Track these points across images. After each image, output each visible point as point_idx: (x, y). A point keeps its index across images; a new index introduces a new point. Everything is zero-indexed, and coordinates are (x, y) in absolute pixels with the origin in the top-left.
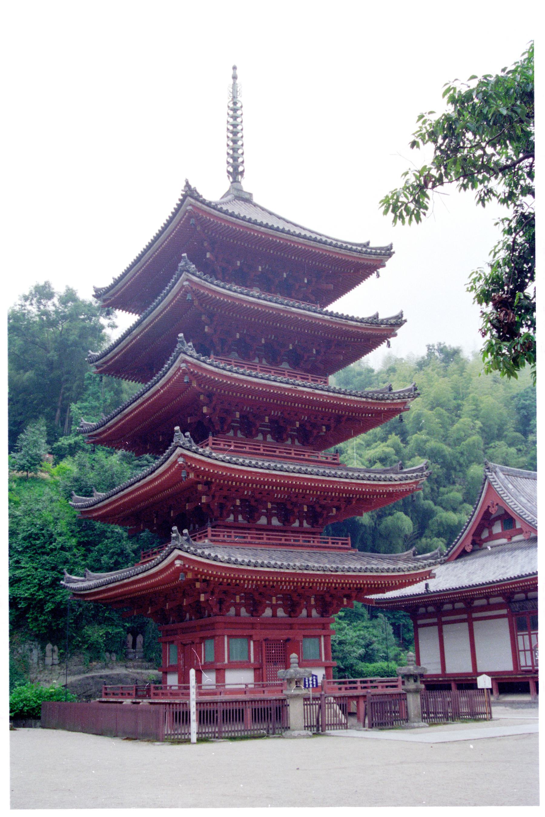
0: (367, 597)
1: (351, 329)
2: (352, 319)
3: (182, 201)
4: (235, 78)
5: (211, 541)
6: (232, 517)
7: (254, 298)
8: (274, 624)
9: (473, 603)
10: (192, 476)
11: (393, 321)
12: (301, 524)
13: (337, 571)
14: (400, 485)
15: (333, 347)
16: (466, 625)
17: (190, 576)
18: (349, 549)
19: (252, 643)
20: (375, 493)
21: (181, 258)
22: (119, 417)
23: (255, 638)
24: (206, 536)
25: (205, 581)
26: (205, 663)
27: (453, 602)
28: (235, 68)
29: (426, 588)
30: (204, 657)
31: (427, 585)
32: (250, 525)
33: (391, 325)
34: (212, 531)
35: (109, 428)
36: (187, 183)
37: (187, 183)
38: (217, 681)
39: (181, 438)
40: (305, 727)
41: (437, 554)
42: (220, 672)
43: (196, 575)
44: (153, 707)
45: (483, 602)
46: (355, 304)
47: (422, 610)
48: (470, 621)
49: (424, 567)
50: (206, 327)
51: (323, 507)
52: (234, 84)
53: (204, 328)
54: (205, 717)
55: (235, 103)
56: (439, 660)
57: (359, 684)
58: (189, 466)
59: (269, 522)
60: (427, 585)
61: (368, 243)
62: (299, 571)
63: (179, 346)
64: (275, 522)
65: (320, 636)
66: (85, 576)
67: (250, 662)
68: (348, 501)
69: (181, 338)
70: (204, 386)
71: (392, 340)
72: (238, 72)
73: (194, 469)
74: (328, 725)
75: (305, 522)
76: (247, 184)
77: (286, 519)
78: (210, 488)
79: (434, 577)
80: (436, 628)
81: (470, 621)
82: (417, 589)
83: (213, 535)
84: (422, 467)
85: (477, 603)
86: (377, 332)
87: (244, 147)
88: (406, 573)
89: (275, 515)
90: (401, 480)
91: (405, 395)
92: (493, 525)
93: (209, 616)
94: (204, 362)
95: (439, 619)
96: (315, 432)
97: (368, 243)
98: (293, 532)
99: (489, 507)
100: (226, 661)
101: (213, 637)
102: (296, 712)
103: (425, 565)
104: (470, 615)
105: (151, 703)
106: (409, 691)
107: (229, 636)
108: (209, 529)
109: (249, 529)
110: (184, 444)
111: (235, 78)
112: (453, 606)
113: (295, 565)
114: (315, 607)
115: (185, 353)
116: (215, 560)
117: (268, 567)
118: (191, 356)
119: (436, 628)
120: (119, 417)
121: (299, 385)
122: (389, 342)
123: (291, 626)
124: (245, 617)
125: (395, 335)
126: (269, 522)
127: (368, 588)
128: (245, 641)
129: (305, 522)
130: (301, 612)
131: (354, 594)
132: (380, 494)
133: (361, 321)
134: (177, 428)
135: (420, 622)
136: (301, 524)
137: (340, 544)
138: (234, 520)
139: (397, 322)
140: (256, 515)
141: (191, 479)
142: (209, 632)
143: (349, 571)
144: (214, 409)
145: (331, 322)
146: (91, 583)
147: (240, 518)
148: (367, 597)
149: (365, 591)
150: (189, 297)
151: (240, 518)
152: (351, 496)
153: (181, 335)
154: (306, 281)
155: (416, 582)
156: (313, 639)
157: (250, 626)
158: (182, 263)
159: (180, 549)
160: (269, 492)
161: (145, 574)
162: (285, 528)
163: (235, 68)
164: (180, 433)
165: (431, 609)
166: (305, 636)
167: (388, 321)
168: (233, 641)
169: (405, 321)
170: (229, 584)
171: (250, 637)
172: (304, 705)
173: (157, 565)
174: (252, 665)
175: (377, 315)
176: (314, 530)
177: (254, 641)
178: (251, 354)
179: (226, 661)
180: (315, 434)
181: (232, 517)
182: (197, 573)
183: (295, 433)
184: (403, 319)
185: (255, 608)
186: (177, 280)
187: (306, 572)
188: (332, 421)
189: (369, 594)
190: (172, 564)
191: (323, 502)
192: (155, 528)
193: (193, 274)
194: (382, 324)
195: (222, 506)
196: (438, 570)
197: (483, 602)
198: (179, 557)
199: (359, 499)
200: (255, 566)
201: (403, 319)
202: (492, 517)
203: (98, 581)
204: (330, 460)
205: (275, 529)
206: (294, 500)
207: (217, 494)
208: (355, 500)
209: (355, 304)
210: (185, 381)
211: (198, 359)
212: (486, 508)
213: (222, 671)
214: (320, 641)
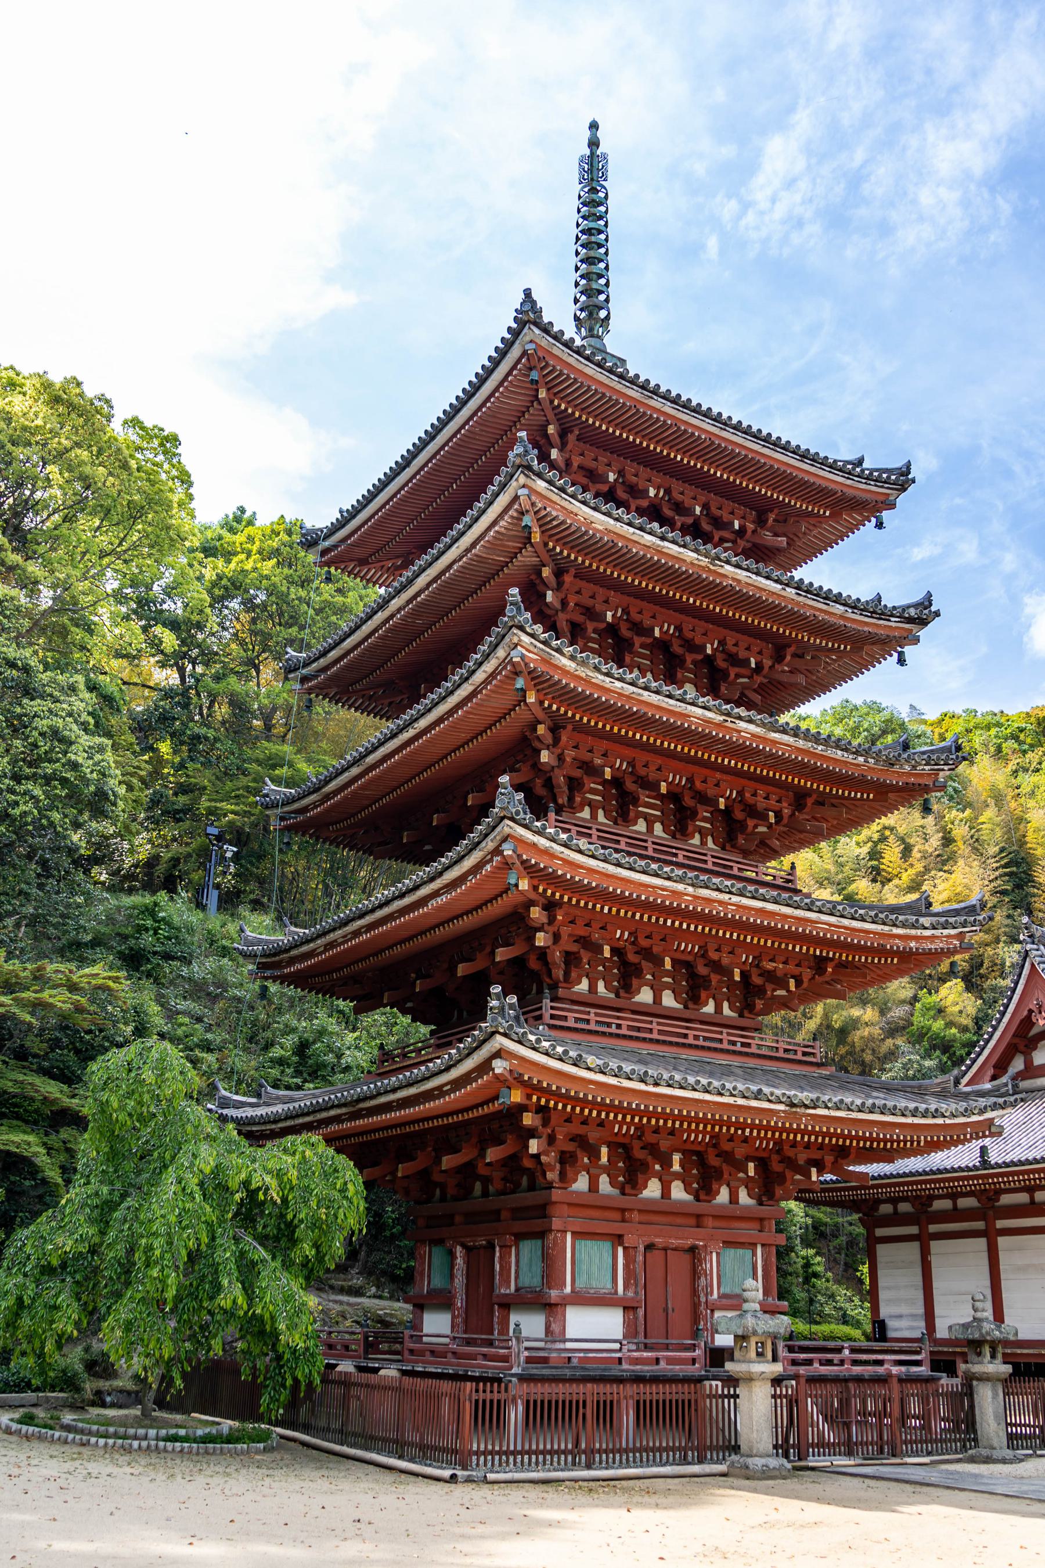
0: (851, 1168)
1: (833, 620)
2: (838, 599)
3: (515, 333)
4: (594, 143)
5: (552, 1027)
6: (584, 985)
7: (647, 540)
8: (664, 1211)
9: (931, 1205)
10: (524, 885)
11: (912, 612)
12: (719, 1009)
13: (814, 1108)
14: (933, 938)
15: (788, 658)
16: (982, 1242)
17: (516, 1096)
18: (819, 1065)
19: (620, 1250)
20: (881, 951)
21: (514, 441)
22: (355, 771)
23: (629, 1240)
24: (539, 1018)
25: (541, 1110)
26: (517, 1290)
27: (954, 1196)
28: (594, 126)
29: (982, 1156)
30: (517, 1278)
31: (983, 1150)
32: (621, 1003)
33: (910, 620)
34: (552, 1008)
35: (327, 797)
36: (528, 293)
37: (528, 293)
38: (548, 1330)
39: (508, 799)
40: (775, 1447)
41: (1006, 1085)
42: (552, 1309)
43: (529, 1097)
44: (407, 1381)
45: (1023, 1198)
46: (845, 571)
47: (886, 1209)
48: (924, 1241)
49: (982, 1112)
50: (549, 593)
51: (770, 976)
52: (592, 153)
53: (545, 595)
54: (540, 1415)
55: (594, 190)
56: (921, 1310)
57: (847, 1352)
58: (523, 862)
59: (657, 999)
60: (983, 1150)
61: (860, 462)
62: (741, 1102)
63: (510, 611)
64: (668, 1000)
65: (753, 1246)
66: (259, 1096)
67: (616, 1292)
68: (820, 964)
69: (513, 596)
70: (550, 706)
71: (908, 650)
72: (599, 134)
73: (531, 870)
74: (813, 1445)
75: (726, 1005)
76: (613, 343)
77: (693, 996)
78: (552, 920)
79: (1000, 1134)
80: (916, 1245)
81: (991, 1236)
82: (961, 1157)
83: (552, 1017)
84: (974, 906)
85: (1006, 1199)
86: (883, 633)
87: (611, 274)
88: (948, 1121)
89: (667, 986)
90: (934, 928)
91: (938, 758)
92: (1035, 1048)
93: (532, 1187)
94: (558, 650)
95: (990, 1225)
96: (751, 823)
97: (860, 462)
98: (702, 1023)
99: (1031, 1011)
100: (568, 1289)
101: (541, 1235)
102: (756, 1413)
103: (985, 1107)
104: (923, 1229)
105: (404, 1373)
106: (984, 1378)
107: (574, 1234)
108: (547, 1003)
109: (619, 1010)
110: (518, 813)
111: (594, 143)
112: (955, 1204)
113: (735, 1088)
114: (748, 1183)
115: (521, 628)
116: (575, 1065)
117: (681, 1088)
118: (532, 636)
119: (982, 1242)
120: (355, 771)
121: (740, 718)
122: (901, 655)
123: (699, 1220)
124: (607, 1197)
125: (916, 641)
126: (657, 999)
127: (864, 1147)
128: (606, 1246)
129: (726, 1005)
130: (718, 1193)
131: (829, 1159)
132: (892, 953)
133: (855, 605)
134: (504, 779)
135: (880, 1232)
136: (719, 1009)
137: (800, 1054)
138: (589, 991)
139: (921, 615)
140: (635, 982)
141: (522, 892)
142: (534, 1222)
143: (838, 1109)
144: (561, 758)
145: (798, 603)
146: (279, 1108)
147: (601, 986)
148: (851, 1168)
149: (852, 1156)
150: (527, 520)
151: (601, 986)
152: (831, 954)
153: (515, 590)
154: (737, 527)
155: (956, 1143)
156: (740, 1251)
157: (617, 1216)
158: (518, 449)
159: (505, 1035)
160: (667, 936)
161: (412, 1091)
162: (688, 1014)
163: (594, 126)
164: (510, 789)
165: (904, 1207)
166: (729, 1244)
167: (904, 610)
168: (584, 1245)
169: (937, 614)
170: (585, 1122)
171: (618, 1239)
172: (774, 1396)
173: (448, 1069)
174: (622, 1299)
175: (879, 598)
176: (743, 1022)
177: (625, 1249)
178: (628, 659)
179: (568, 1289)
180: (750, 829)
181: (584, 985)
182: (530, 1088)
183: (708, 826)
184: (933, 609)
185: (632, 1176)
186: (503, 486)
187: (754, 1103)
188: (785, 804)
189: (854, 1164)
190: (485, 1066)
191: (770, 966)
192: (409, 1005)
193: (540, 475)
194: (892, 616)
195: (571, 959)
196: (1008, 1119)
197: (1023, 1198)
198: (498, 1054)
199: (842, 965)
200: (656, 1084)
201: (933, 609)
202: (1034, 1031)
203: (285, 1107)
204: (779, 882)
205: (668, 1015)
206: (714, 955)
207: (565, 931)
208: (837, 966)
209: (845, 571)
210: (518, 686)
211: (545, 643)
212: (1025, 1013)
213: (559, 1309)
214: (754, 1254)
